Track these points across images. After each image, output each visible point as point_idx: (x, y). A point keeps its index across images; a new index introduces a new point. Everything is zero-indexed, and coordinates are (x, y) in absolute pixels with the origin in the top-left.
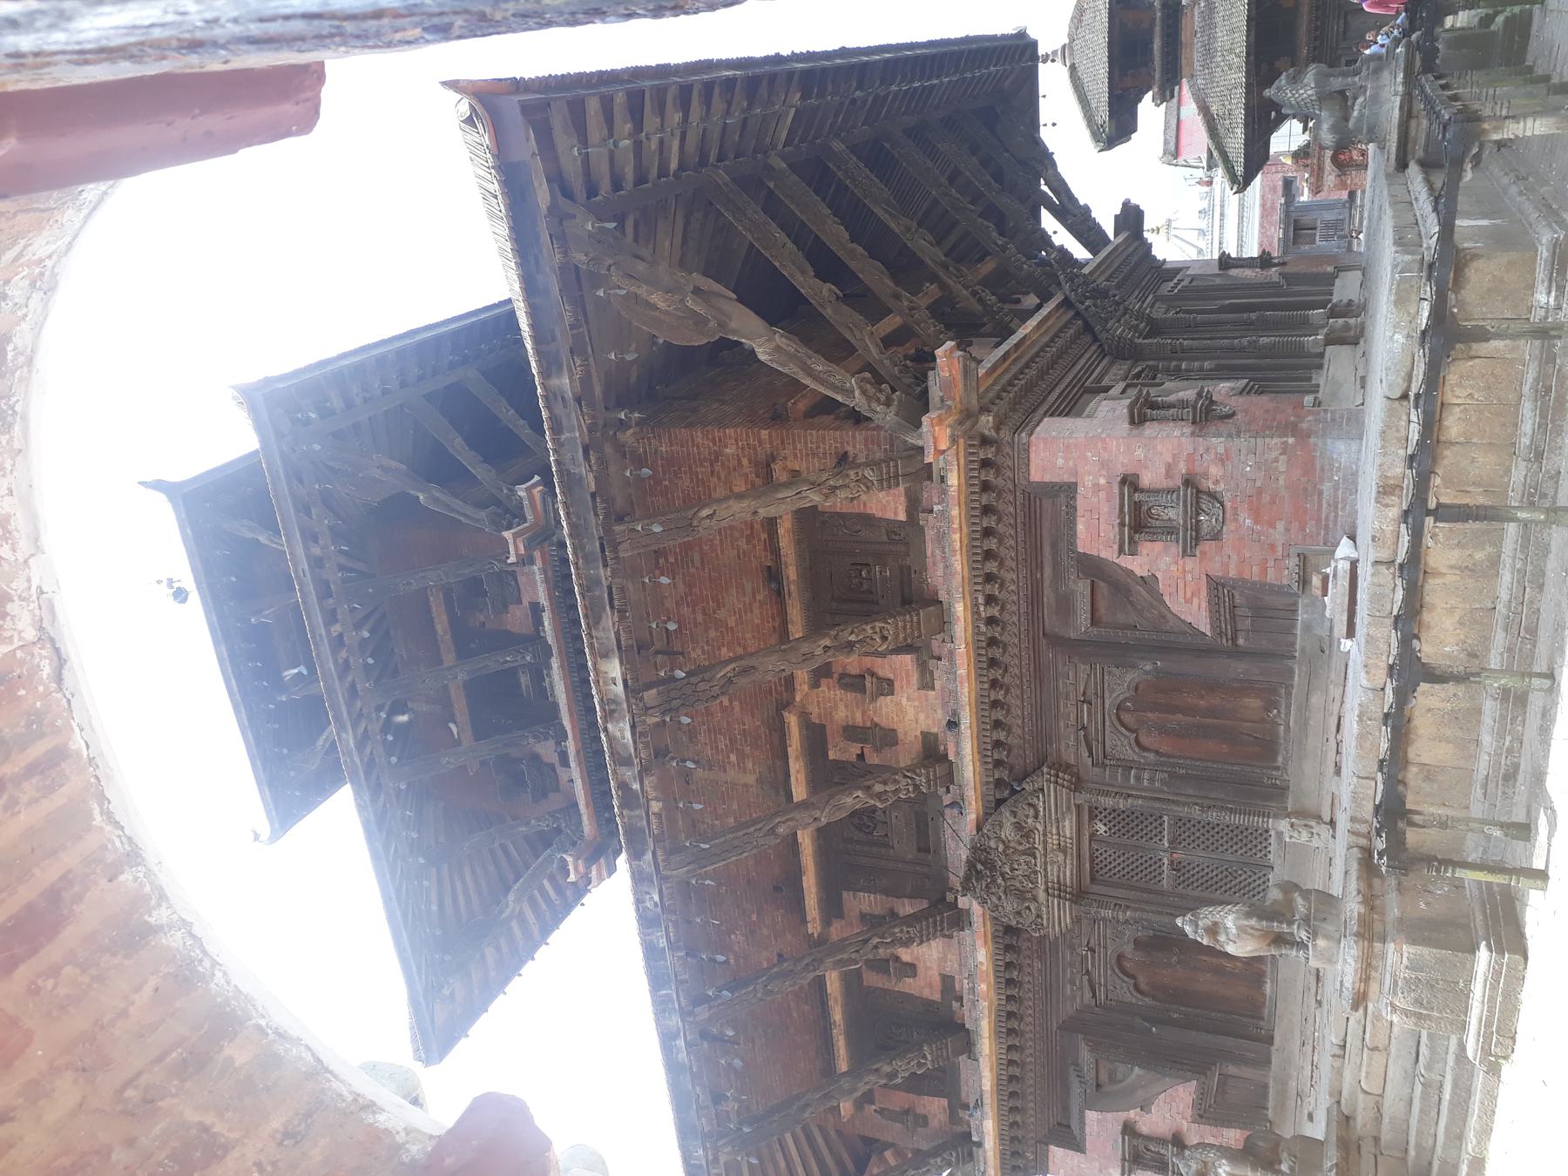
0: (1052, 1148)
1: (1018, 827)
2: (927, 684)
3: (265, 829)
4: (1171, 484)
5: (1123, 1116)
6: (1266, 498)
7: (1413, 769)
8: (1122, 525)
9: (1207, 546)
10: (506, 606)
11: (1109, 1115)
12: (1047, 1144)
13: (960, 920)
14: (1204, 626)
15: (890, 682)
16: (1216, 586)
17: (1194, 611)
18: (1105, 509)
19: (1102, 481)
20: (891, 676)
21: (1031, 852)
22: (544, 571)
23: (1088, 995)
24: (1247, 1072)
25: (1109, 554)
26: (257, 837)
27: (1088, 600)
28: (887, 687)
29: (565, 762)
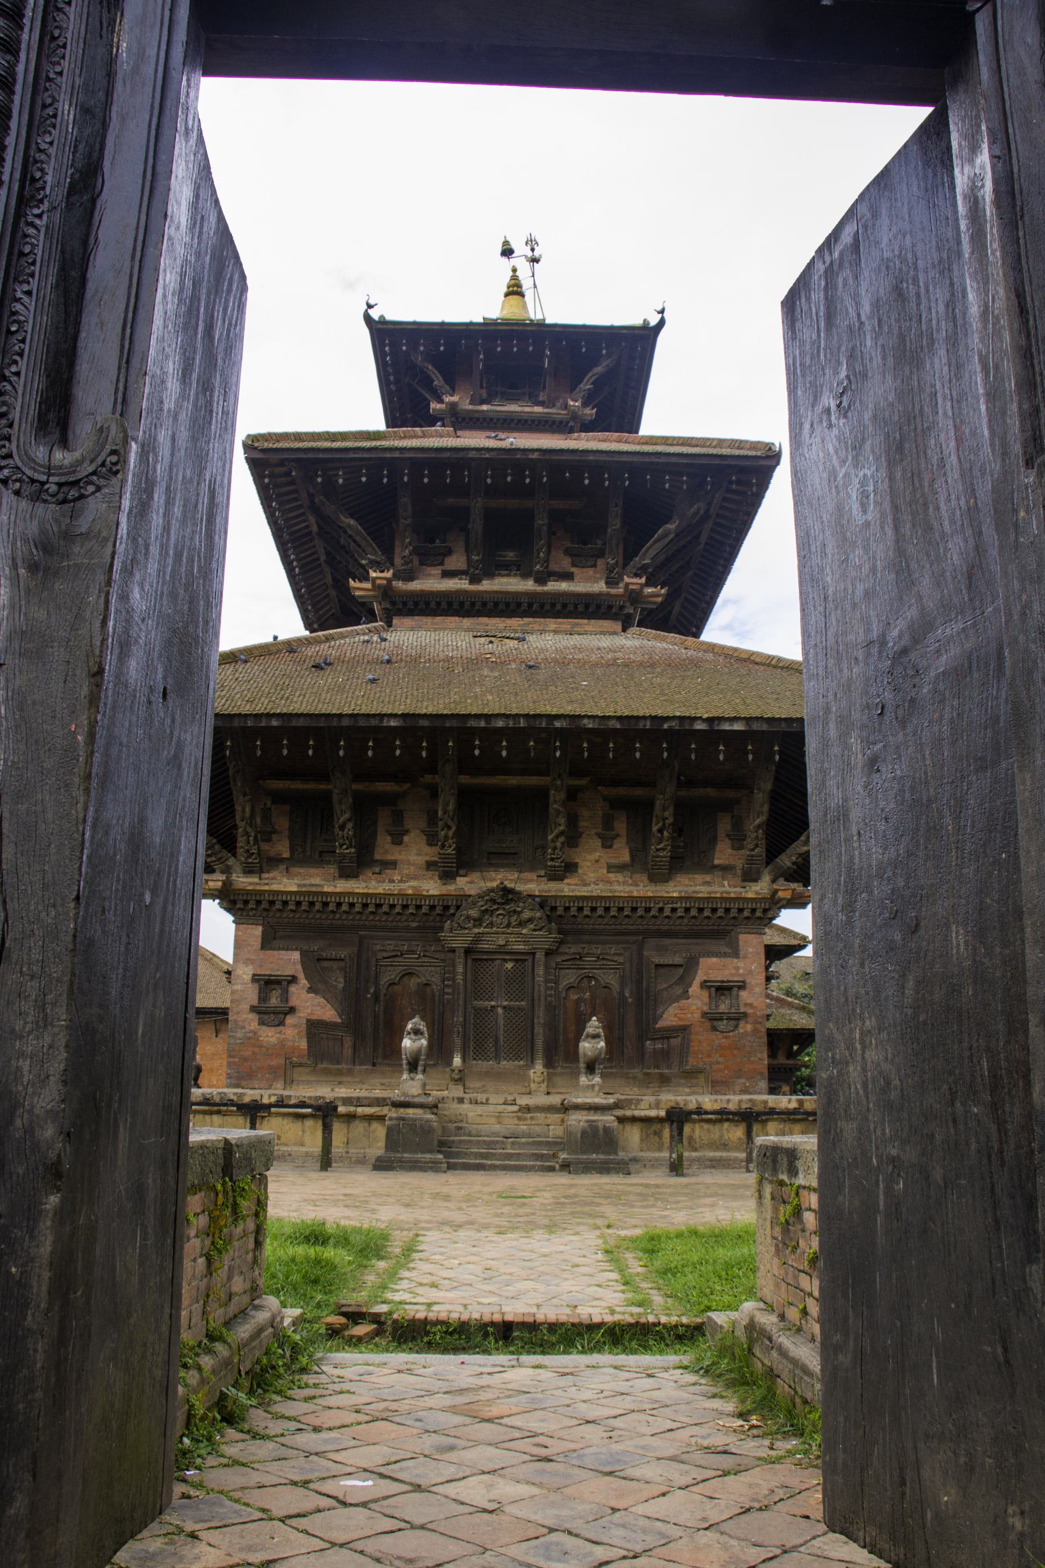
0: (260, 928)
1: (530, 920)
2: (611, 868)
3: (375, 314)
4: (741, 1006)
5: (301, 976)
6: (735, 1052)
7: (659, 1126)
8: (723, 982)
9: (708, 1024)
10: (571, 555)
11: (299, 967)
12: (263, 925)
13: (447, 876)
14: (660, 1024)
15: (610, 847)
16: (683, 1030)
17: (670, 1017)
18: (726, 972)
19: (741, 971)
20: (615, 847)
21: (508, 926)
22: (600, 594)
23: (385, 955)
24: (348, 1051)
25: (700, 976)
26: (370, 306)
27: (666, 962)
28: (607, 843)
29: (447, 574)
